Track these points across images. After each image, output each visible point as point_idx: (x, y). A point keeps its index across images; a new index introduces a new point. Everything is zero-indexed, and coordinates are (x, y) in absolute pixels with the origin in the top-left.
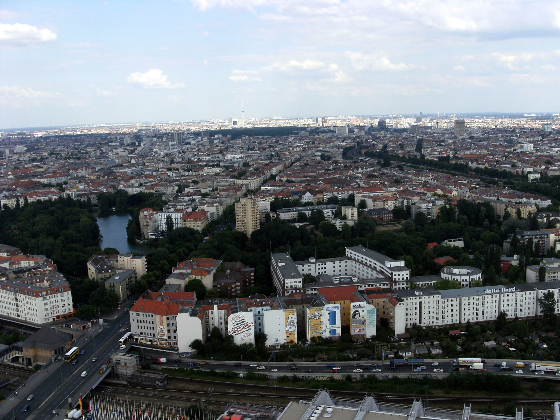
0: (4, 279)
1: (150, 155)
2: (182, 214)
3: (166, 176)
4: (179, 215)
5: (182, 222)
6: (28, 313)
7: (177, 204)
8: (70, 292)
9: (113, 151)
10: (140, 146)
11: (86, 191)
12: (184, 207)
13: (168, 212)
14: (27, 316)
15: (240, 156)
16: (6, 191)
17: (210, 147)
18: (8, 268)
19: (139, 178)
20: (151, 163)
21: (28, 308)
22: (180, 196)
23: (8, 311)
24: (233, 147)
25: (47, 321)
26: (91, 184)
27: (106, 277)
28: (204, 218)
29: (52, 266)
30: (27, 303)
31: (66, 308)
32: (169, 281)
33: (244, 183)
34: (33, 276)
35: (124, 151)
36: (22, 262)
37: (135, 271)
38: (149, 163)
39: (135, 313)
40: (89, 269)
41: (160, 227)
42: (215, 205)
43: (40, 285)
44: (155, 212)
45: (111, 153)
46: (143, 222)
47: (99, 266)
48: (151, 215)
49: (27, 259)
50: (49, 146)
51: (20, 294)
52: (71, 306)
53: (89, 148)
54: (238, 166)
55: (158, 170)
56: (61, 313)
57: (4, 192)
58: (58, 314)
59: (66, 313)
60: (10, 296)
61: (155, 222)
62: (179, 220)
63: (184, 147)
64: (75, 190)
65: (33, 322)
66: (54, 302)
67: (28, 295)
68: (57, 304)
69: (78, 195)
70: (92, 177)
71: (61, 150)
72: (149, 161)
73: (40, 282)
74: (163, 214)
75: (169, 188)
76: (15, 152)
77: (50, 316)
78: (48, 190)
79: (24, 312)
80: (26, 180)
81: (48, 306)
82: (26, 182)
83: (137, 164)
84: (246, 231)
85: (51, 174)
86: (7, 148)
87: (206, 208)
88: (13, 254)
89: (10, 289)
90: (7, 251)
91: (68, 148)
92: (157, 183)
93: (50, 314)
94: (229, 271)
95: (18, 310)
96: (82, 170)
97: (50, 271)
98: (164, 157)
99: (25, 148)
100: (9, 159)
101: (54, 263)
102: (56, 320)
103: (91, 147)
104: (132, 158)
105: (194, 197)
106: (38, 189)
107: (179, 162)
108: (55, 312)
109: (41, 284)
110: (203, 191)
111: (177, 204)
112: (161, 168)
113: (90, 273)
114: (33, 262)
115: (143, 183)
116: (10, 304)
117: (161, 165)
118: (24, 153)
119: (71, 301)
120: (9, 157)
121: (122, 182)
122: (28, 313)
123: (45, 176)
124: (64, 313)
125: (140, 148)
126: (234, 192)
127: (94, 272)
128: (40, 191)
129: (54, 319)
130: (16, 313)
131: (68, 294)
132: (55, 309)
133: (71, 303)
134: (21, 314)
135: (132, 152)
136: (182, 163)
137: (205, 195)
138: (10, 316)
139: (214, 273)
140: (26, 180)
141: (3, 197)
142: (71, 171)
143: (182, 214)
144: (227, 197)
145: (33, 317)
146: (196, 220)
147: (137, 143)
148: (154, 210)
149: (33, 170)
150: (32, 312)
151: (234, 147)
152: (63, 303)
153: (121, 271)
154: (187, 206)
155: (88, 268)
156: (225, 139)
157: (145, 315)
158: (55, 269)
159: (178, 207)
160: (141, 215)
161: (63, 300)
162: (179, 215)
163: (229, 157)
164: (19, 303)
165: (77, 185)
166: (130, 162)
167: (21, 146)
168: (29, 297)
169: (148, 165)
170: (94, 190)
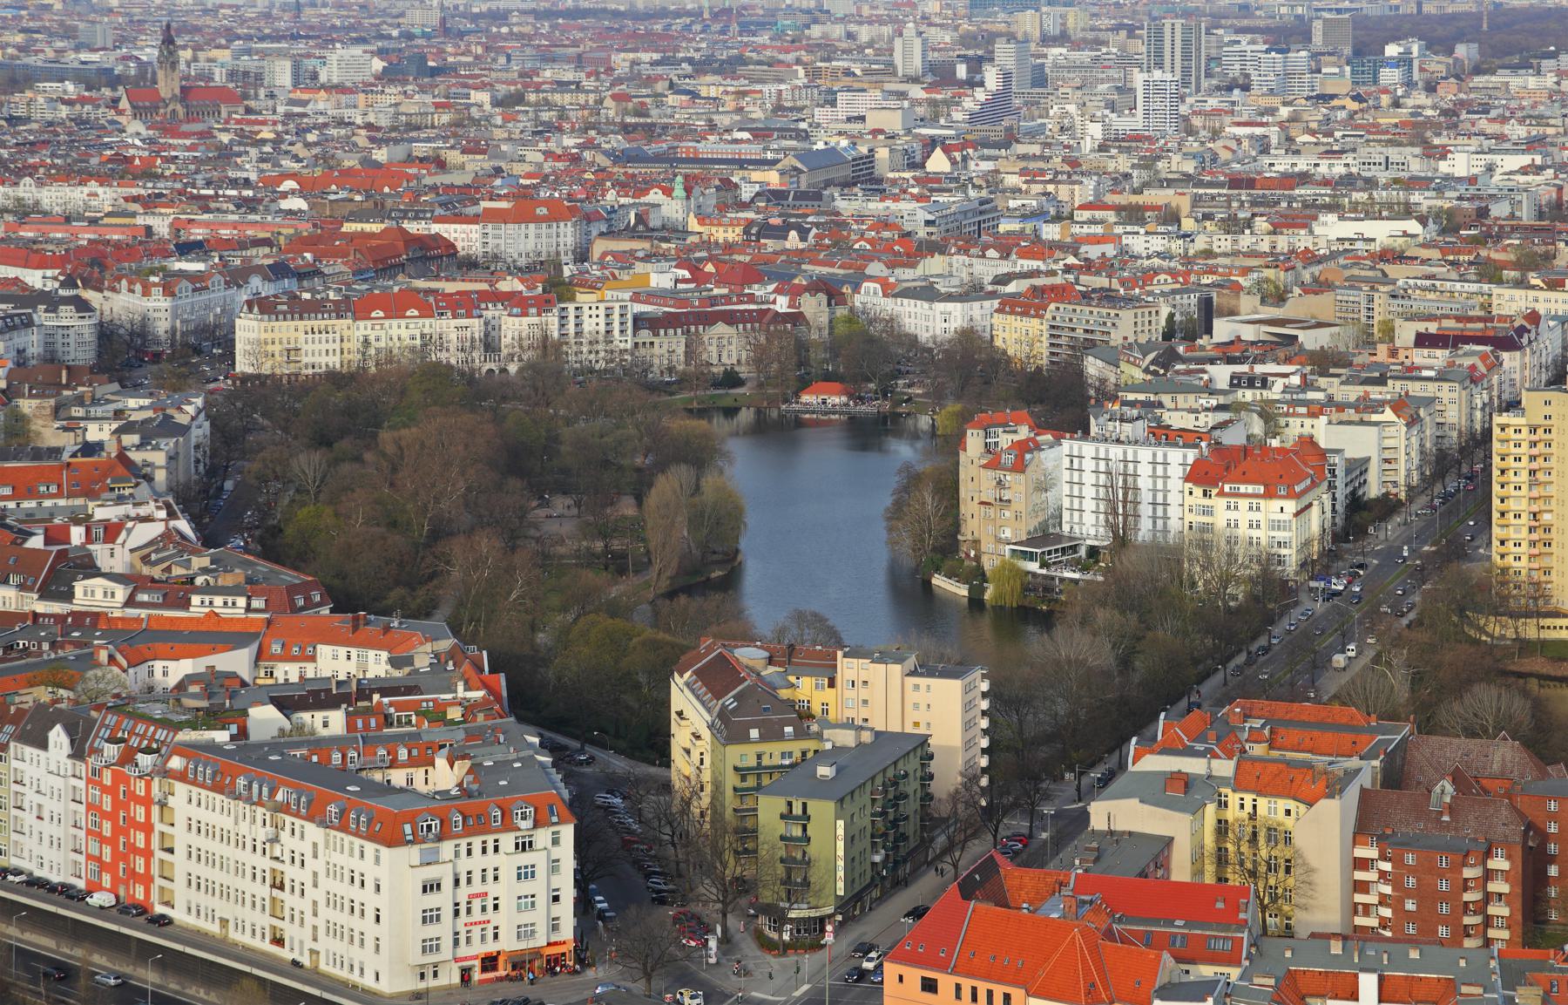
0: (221, 736)
1: (1032, 135)
2: (1192, 455)
3: (1110, 250)
4: (1179, 459)
5: (1189, 500)
6: (333, 930)
7: (1166, 399)
8: (567, 832)
9: (833, 103)
10: (982, 84)
11: (685, 302)
12: (1208, 420)
13: (1118, 441)
14: (325, 944)
15: (1525, 160)
16: (266, 278)
17: (1355, 106)
18: (247, 677)
19: (966, 253)
20: (1031, 176)
21: (332, 901)
22: (1184, 360)
23: (224, 909)
24: (1485, 109)
25: (431, 983)
26: (710, 268)
27: (766, 761)
28: (1314, 485)
29: (485, 686)
30: (332, 871)
31: (539, 917)
32: (1110, 814)
33: (1541, 308)
34: (379, 728)
35: (892, 103)
36: (324, 651)
37: (924, 741)
38: (1023, 172)
39: (914, 975)
40: (680, 714)
41: (1066, 516)
42: (1375, 417)
43: (410, 781)
44: (1049, 437)
45: (820, 114)
46: (975, 481)
47: (729, 701)
48: (1022, 448)
49: (354, 638)
50: (502, 60)
51: (298, 822)
52: (566, 911)
53: (709, 78)
54: (1512, 216)
55: (1071, 217)
56: (509, 943)
57: (256, 282)
58: (491, 947)
59: (532, 944)
60: (244, 828)
61: (1043, 487)
62: (1176, 483)
63: (1213, 102)
64: (627, 296)
65: (355, 977)
66: (476, 877)
67: (343, 828)
68: (492, 889)
69: (639, 322)
70: (721, 234)
71: (560, 83)
72: (1023, 164)
73: (412, 762)
74: (1088, 449)
75: (1127, 316)
76: (323, 78)
77: (446, 951)
78: (484, 286)
79: (308, 916)
80: (374, 227)
81: (442, 900)
82: (372, 235)
83: (956, 182)
84: (1547, 572)
85: (504, 205)
86: (281, 54)
87: (1323, 432)
88: (285, 603)
89: (249, 787)
90: (250, 587)
91: (597, 74)
92: (1058, 280)
93: (447, 943)
94: (1449, 788)
95: (276, 909)
96: (668, 192)
97: (470, 708)
98: (1102, 148)
99: (378, 65)
100: (289, 116)
101: (494, 670)
102: (477, 976)
103: (717, 78)
104: (931, 144)
105: (1259, 369)
106: (437, 278)
107: (1187, 179)
108: (476, 932)
109: (418, 774)
110: (1311, 340)
111: (1166, 399)
112: (1084, 207)
113: (680, 737)
114: (384, 655)
115: (988, 279)
116: (239, 870)
117: (1085, 190)
118: (367, 88)
119: (566, 884)
120: (292, 102)
121: (875, 268)
122: (333, 930)
123: (471, 210)
124: (522, 945)
125: (980, 95)
126: (1484, 357)
127: (706, 734)
128: (450, 287)
129: (466, 974)
130: (265, 921)
131: (555, 842)
132: (477, 915)
133: (568, 893)
134: (289, 930)
135: (936, 111)
136: (1201, 184)
137: (1324, 362)
138: (234, 936)
139: (1363, 791)
140: (374, 227)
141: (250, 304)
142: (611, 196)
143: (1192, 455)
144: (1442, 377)
145: (356, 954)
146: (1269, 495)
147: (962, 71)
148: (1039, 426)
149: (409, 178)
150: (355, 922)
151: (1493, 113)
152: (527, 887)
153: (847, 738)
154: (1224, 416)
155: (674, 708)
156: (1438, 65)
157: (966, 993)
158: (498, 698)
159: (1176, 420)
160: (974, 442)
161: (525, 874)
162: (1179, 459)
163: (1460, 164)
164: (291, 872)
165: (640, 267)
166: (923, 166)
167: (357, 51)
168: (348, 838)
169: (1016, 191)
170: (727, 299)
